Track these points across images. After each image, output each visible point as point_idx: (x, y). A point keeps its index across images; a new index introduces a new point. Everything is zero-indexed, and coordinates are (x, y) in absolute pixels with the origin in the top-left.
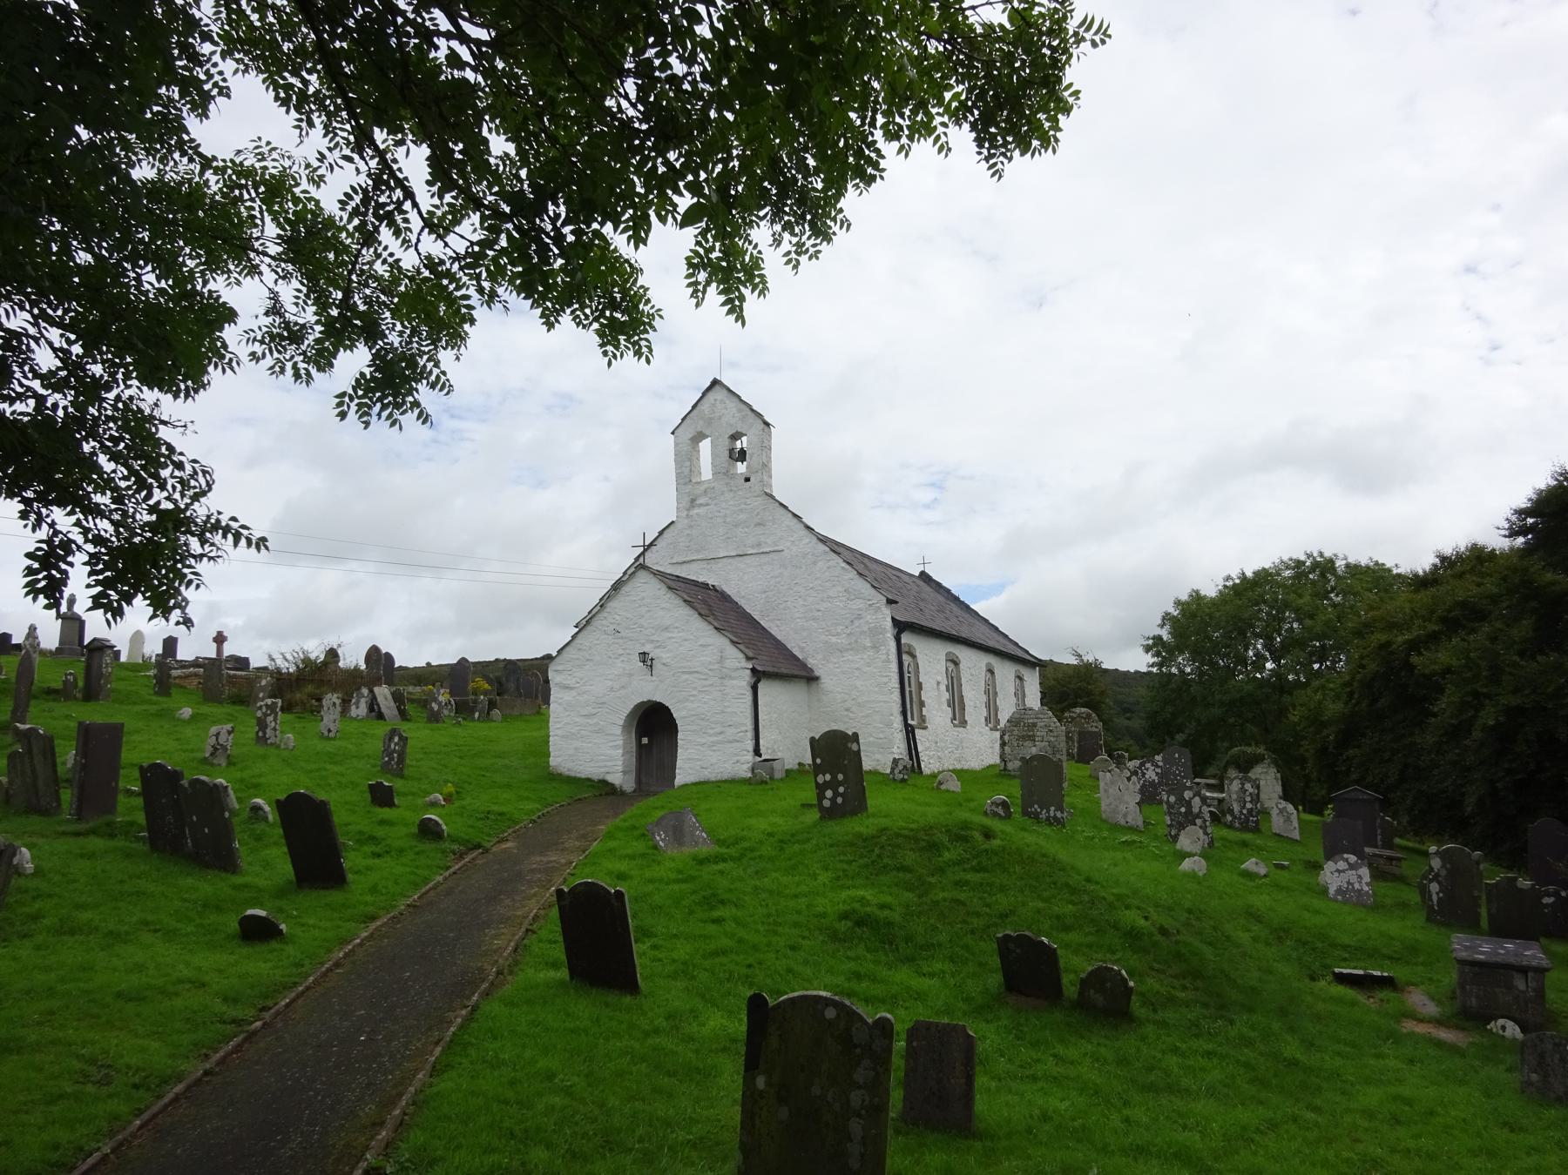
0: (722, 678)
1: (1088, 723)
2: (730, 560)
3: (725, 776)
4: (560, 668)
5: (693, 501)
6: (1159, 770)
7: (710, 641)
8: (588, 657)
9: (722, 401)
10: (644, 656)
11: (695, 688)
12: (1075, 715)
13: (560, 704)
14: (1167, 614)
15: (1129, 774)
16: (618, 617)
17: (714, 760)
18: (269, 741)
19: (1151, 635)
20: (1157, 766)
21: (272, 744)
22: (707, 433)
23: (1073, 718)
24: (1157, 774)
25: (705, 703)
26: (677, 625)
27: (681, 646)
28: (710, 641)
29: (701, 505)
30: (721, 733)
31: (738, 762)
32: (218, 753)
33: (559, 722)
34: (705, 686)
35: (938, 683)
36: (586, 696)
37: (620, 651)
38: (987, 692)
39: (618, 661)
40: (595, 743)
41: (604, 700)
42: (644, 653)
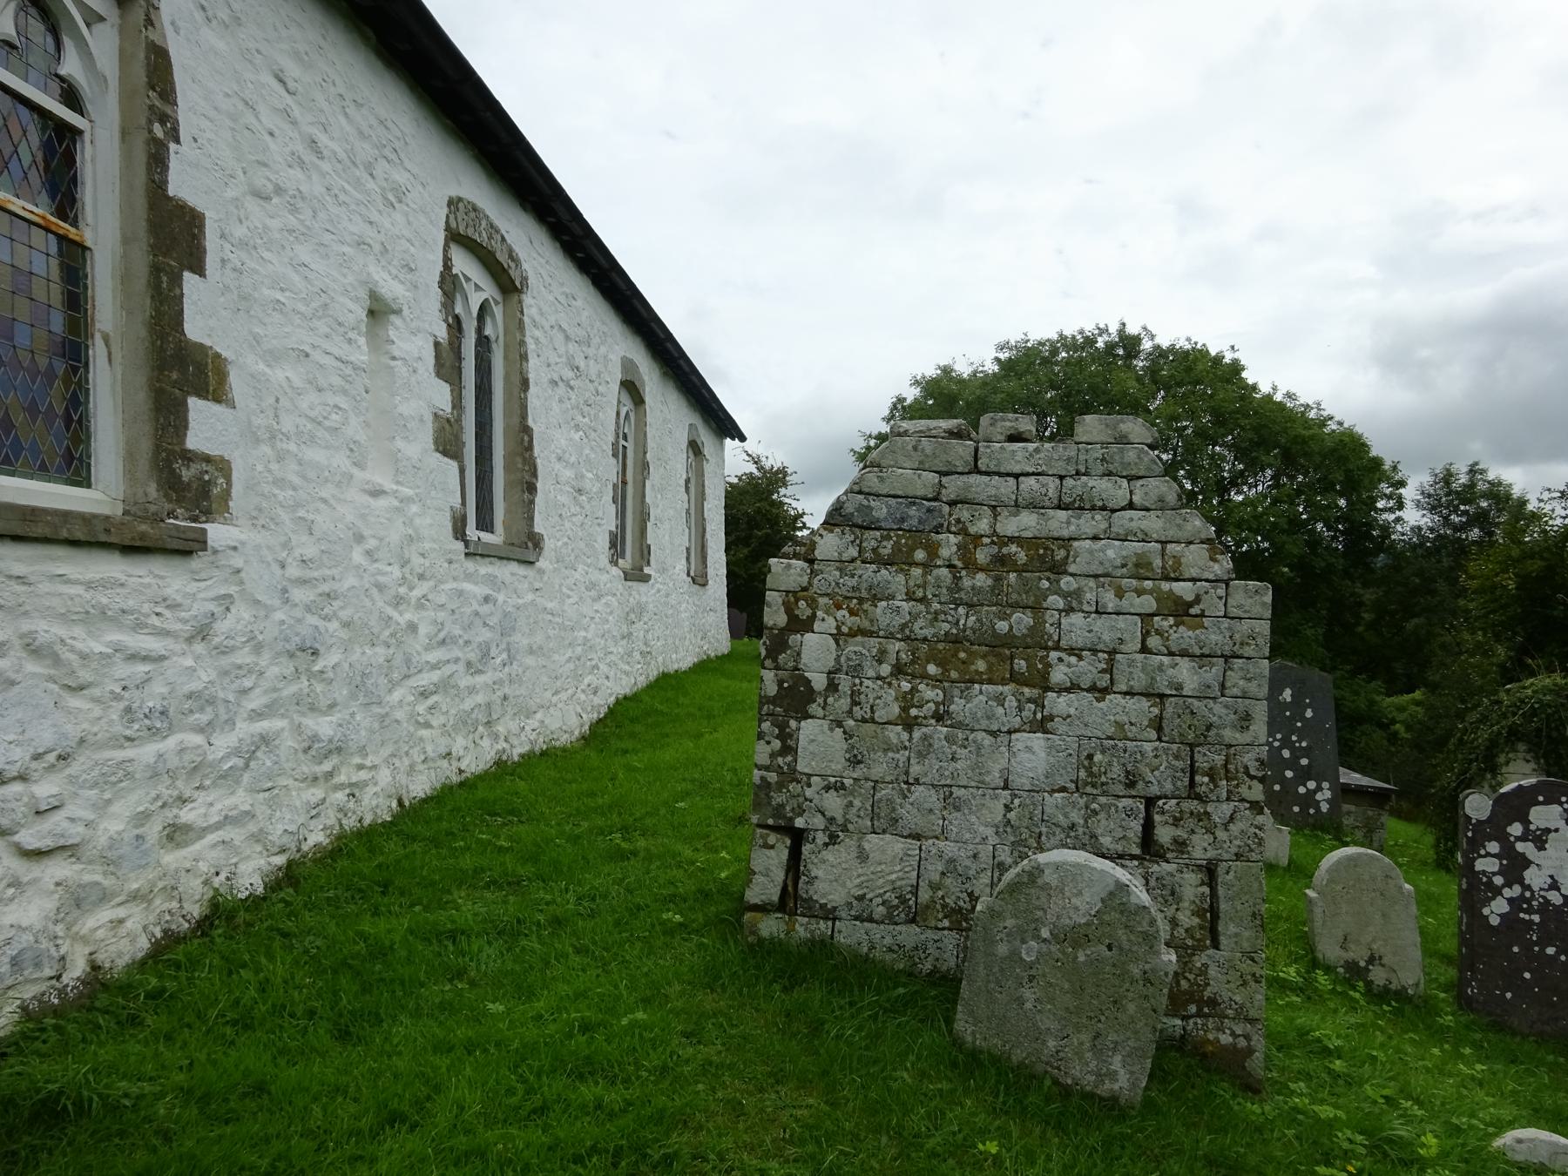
14: (901, 400)
19: (875, 433)
35: (378, 311)
38: (619, 453)
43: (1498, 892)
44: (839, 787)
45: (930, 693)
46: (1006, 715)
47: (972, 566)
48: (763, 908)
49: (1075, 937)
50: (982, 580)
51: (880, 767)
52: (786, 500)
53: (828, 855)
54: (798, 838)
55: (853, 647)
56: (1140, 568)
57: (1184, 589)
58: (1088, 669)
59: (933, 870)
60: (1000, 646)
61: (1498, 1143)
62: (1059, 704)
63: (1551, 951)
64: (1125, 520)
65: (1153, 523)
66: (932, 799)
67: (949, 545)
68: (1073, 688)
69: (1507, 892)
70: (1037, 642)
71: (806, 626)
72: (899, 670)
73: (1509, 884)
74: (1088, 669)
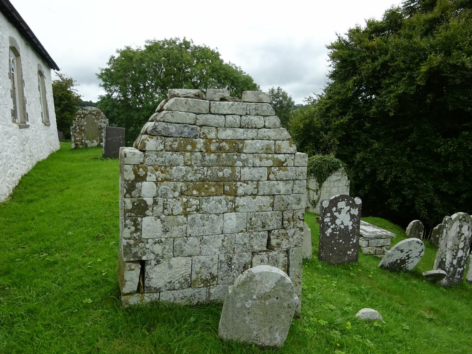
1: (98, 119)
12: (86, 112)
14: (113, 57)
19: (104, 68)
23: (85, 115)
24: (352, 216)
38: (11, 77)
43: (329, 227)
44: (160, 242)
45: (194, 202)
46: (222, 207)
47: (209, 151)
48: (131, 294)
49: (265, 297)
50: (213, 156)
51: (176, 232)
52: (74, 91)
53: (157, 269)
54: (143, 264)
55: (164, 186)
56: (267, 150)
57: (281, 157)
59: (197, 267)
60: (220, 182)
61: (357, 315)
62: (240, 201)
63: (341, 241)
65: (271, 133)
66: (196, 241)
67: (200, 143)
68: (245, 195)
69: (332, 227)
70: (233, 179)
71: (143, 179)
72: (182, 194)
73: (332, 225)
74: (250, 188)
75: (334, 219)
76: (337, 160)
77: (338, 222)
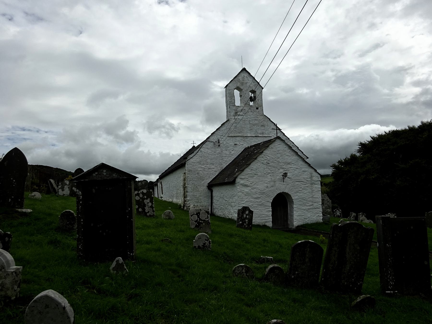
0: (312, 184)
2: (252, 138)
3: (314, 222)
4: (243, 177)
5: (236, 113)
6: (340, 212)
7: (307, 169)
8: (256, 173)
9: (246, 77)
10: (285, 175)
11: (301, 188)
13: (243, 193)
15: (394, 216)
16: (268, 157)
17: (309, 216)
18: (148, 214)
20: (340, 211)
21: (150, 216)
22: (242, 88)
24: (340, 213)
25: (305, 193)
26: (293, 162)
27: (295, 171)
28: (307, 169)
29: (239, 115)
30: (312, 205)
31: (318, 216)
32: (201, 225)
33: (243, 201)
34: (305, 187)
36: (255, 190)
37: (269, 171)
39: (268, 175)
40: (260, 210)
41: (264, 191)
42: (285, 173)
49: (329, 212)
56: (327, 200)
58: (325, 204)
62: (325, 205)
64: (326, 198)
65: (327, 198)
70: (324, 203)
74: (325, 204)
75: (336, 213)
76: (337, 206)
77: (337, 214)
